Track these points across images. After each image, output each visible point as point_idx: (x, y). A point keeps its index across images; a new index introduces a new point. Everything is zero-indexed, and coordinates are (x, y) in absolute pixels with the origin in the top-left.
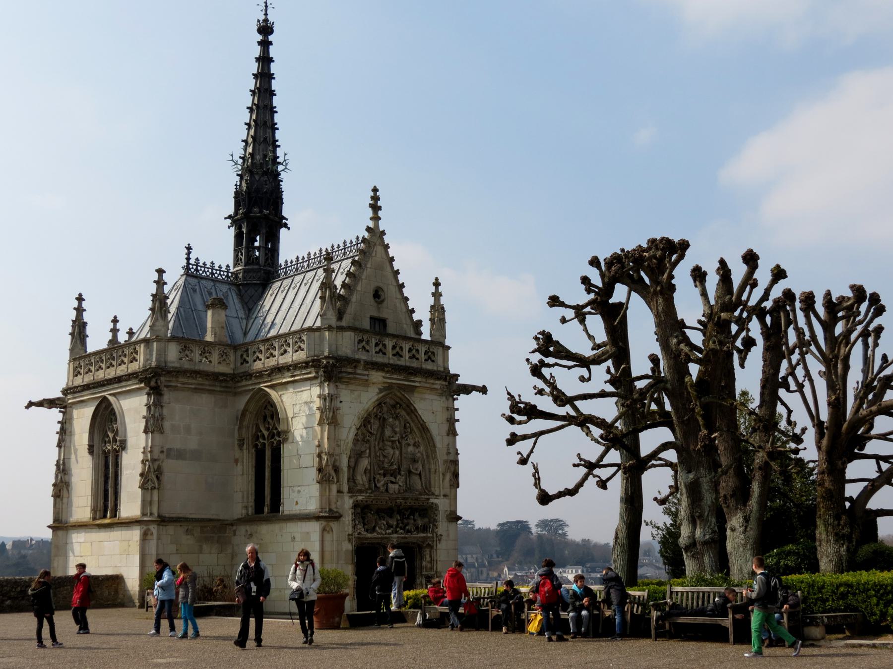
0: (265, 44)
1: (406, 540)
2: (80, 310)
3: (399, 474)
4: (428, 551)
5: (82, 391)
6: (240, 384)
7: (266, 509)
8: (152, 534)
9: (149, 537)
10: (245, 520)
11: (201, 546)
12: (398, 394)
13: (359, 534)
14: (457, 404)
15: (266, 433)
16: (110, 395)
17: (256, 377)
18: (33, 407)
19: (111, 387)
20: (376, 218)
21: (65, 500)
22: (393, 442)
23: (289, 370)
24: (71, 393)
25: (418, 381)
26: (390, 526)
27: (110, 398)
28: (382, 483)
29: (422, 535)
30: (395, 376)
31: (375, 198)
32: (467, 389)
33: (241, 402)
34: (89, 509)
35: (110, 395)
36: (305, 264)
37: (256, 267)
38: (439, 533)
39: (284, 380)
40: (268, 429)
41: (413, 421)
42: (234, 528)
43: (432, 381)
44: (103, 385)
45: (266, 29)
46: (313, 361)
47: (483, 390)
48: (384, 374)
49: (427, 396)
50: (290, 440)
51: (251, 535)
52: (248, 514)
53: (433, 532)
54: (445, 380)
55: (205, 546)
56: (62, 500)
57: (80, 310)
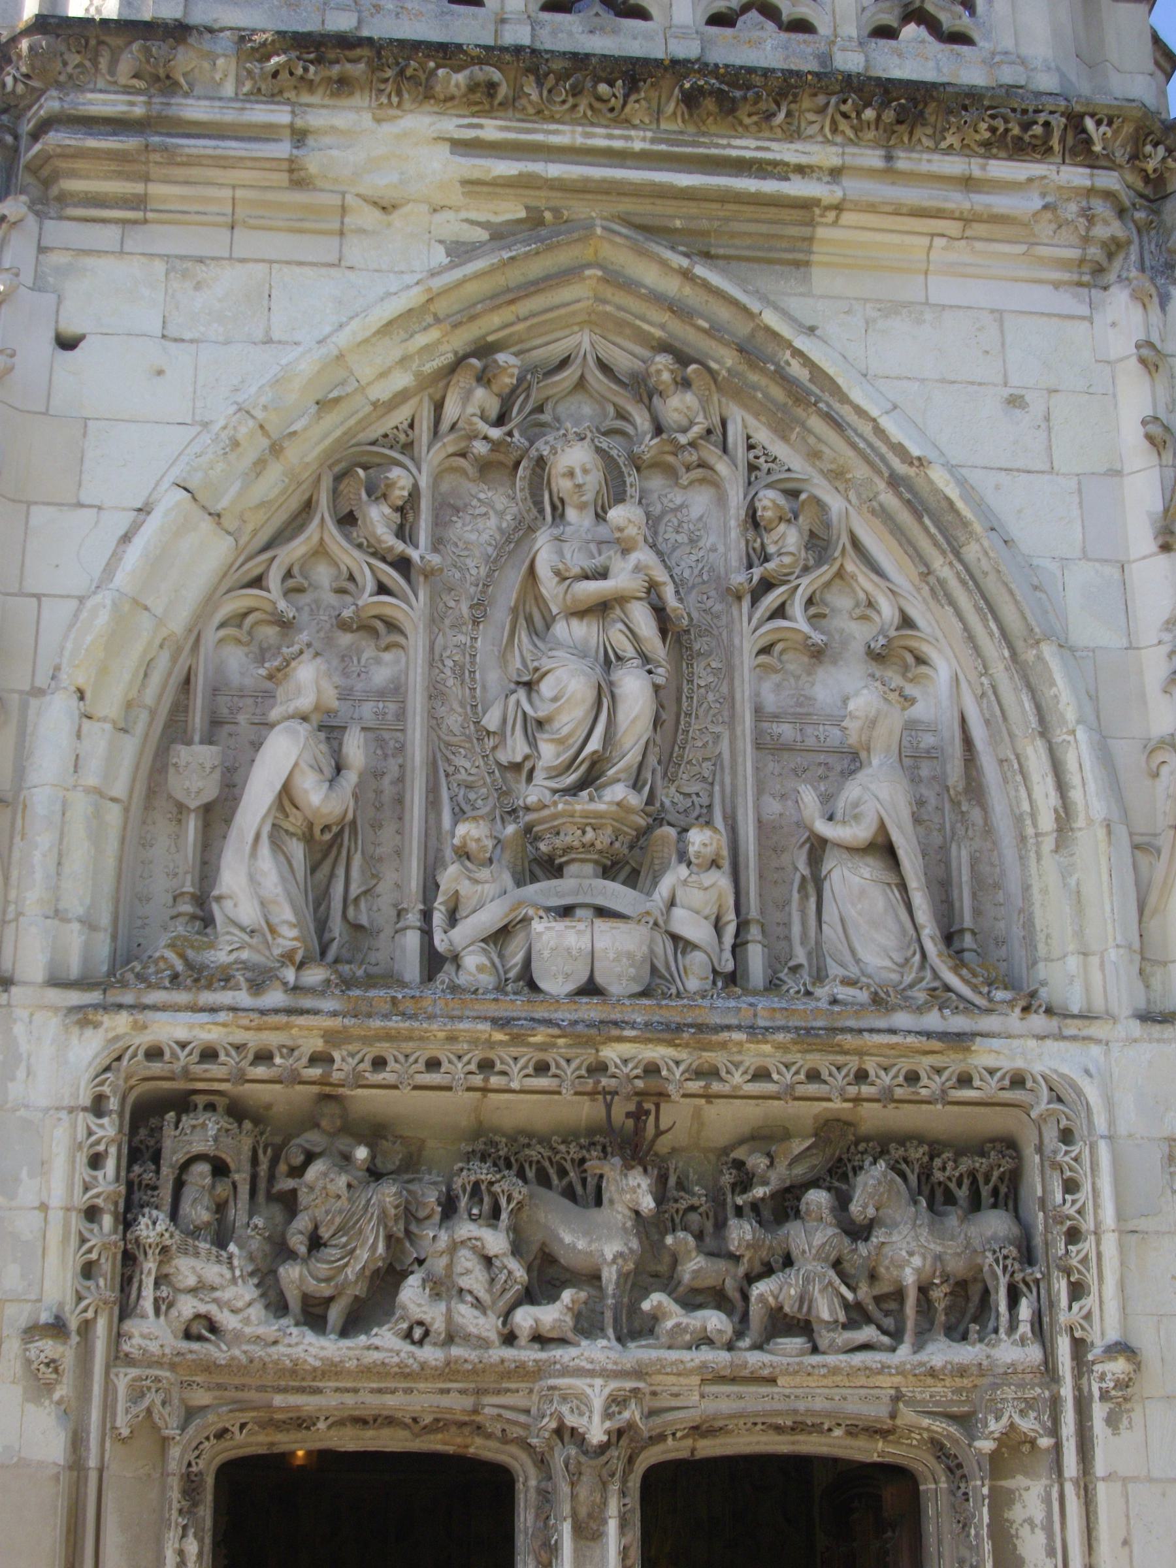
1: (754, 1399)
3: (683, 857)
4: (1031, 1497)
12: (650, 275)
13: (203, 1328)
22: (602, 609)
25: (812, 157)
26: (547, 1276)
28: (488, 917)
29: (942, 1353)
30: (565, 135)
38: (1106, 1329)
41: (837, 476)
43: (954, 165)
48: (452, 125)
49: (942, 289)
53: (1041, 1330)
54: (1080, 149)
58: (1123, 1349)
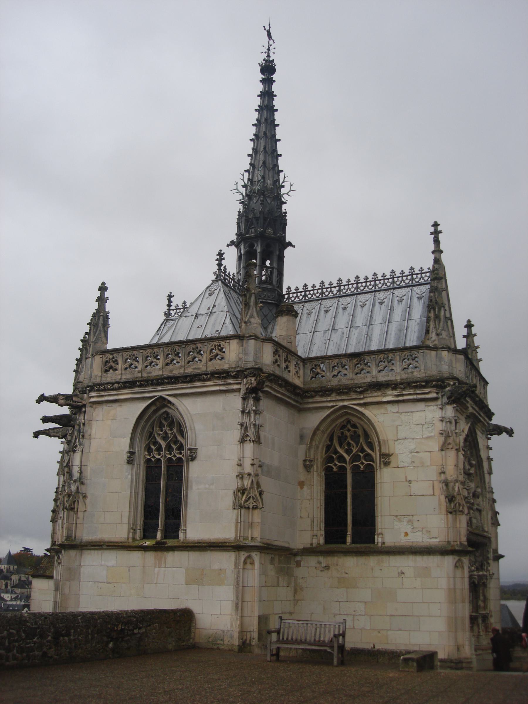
0: (268, 81)
2: (102, 300)
5: (119, 389)
6: (310, 400)
7: (349, 539)
8: (252, 563)
9: (248, 566)
10: (311, 551)
11: (278, 578)
14: (491, 443)
16: (168, 395)
17: (339, 394)
18: (45, 402)
19: (173, 386)
20: (437, 251)
21: (80, 514)
23: (394, 389)
24: (98, 390)
27: (170, 399)
31: (436, 233)
32: (499, 430)
33: (313, 420)
34: (125, 527)
35: (168, 395)
36: (335, 290)
39: (385, 399)
40: (348, 452)
42: (298, 558)
44: (158, 384)
45: (268, 69)
46: (438, 380)
47: (510, 432)
50: (393, 464)
51: (327, 568)
52: (319, 544)
55: (280, 579)
56: (77, 514)
57: (102, 300)
58: (493, 574)
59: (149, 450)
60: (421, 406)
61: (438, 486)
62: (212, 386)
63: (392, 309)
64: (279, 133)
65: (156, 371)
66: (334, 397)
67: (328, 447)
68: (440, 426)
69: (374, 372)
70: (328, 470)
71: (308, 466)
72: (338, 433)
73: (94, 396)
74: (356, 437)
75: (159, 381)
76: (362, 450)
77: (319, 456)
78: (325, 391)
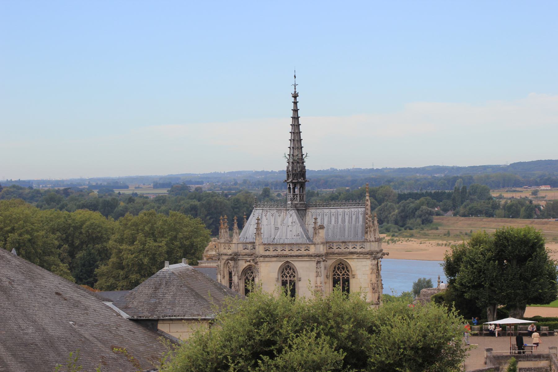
0: (295, 103)
15: (341, 275)
33: (330, 262)
37: (303, 202)
40: (341, 273)
45: (295, 96)
59: (283, 277)
60: (365, 260)
61: (370, 285)
62: (306, 259)
63: (352, 218)
64: (301, 128)
65: (287, 252)
66: (337, 255)
67: (334, 271)
68: (371, 267)
69: (350, 247)
70: (334, 278)
71: (327, 277)
72: (337, 266)
73: (262, 259)
74: (343, 268)
75: (286, 256)
76: (345, 272)
77: (331, 274)
78: (333, 254)
